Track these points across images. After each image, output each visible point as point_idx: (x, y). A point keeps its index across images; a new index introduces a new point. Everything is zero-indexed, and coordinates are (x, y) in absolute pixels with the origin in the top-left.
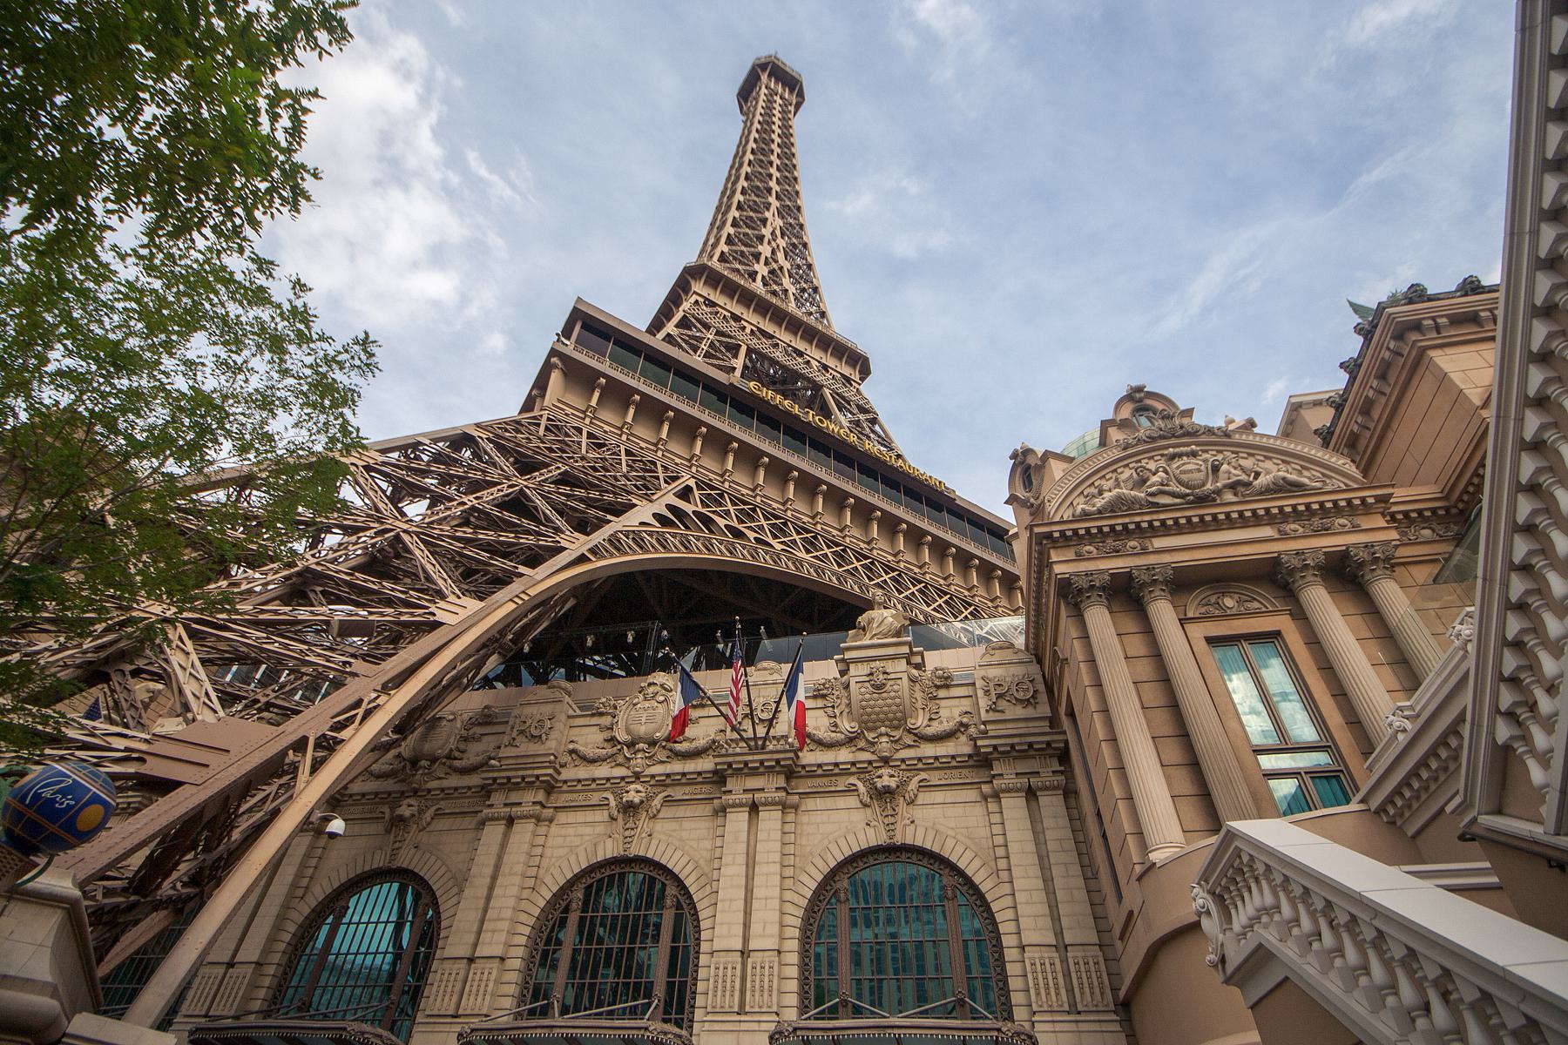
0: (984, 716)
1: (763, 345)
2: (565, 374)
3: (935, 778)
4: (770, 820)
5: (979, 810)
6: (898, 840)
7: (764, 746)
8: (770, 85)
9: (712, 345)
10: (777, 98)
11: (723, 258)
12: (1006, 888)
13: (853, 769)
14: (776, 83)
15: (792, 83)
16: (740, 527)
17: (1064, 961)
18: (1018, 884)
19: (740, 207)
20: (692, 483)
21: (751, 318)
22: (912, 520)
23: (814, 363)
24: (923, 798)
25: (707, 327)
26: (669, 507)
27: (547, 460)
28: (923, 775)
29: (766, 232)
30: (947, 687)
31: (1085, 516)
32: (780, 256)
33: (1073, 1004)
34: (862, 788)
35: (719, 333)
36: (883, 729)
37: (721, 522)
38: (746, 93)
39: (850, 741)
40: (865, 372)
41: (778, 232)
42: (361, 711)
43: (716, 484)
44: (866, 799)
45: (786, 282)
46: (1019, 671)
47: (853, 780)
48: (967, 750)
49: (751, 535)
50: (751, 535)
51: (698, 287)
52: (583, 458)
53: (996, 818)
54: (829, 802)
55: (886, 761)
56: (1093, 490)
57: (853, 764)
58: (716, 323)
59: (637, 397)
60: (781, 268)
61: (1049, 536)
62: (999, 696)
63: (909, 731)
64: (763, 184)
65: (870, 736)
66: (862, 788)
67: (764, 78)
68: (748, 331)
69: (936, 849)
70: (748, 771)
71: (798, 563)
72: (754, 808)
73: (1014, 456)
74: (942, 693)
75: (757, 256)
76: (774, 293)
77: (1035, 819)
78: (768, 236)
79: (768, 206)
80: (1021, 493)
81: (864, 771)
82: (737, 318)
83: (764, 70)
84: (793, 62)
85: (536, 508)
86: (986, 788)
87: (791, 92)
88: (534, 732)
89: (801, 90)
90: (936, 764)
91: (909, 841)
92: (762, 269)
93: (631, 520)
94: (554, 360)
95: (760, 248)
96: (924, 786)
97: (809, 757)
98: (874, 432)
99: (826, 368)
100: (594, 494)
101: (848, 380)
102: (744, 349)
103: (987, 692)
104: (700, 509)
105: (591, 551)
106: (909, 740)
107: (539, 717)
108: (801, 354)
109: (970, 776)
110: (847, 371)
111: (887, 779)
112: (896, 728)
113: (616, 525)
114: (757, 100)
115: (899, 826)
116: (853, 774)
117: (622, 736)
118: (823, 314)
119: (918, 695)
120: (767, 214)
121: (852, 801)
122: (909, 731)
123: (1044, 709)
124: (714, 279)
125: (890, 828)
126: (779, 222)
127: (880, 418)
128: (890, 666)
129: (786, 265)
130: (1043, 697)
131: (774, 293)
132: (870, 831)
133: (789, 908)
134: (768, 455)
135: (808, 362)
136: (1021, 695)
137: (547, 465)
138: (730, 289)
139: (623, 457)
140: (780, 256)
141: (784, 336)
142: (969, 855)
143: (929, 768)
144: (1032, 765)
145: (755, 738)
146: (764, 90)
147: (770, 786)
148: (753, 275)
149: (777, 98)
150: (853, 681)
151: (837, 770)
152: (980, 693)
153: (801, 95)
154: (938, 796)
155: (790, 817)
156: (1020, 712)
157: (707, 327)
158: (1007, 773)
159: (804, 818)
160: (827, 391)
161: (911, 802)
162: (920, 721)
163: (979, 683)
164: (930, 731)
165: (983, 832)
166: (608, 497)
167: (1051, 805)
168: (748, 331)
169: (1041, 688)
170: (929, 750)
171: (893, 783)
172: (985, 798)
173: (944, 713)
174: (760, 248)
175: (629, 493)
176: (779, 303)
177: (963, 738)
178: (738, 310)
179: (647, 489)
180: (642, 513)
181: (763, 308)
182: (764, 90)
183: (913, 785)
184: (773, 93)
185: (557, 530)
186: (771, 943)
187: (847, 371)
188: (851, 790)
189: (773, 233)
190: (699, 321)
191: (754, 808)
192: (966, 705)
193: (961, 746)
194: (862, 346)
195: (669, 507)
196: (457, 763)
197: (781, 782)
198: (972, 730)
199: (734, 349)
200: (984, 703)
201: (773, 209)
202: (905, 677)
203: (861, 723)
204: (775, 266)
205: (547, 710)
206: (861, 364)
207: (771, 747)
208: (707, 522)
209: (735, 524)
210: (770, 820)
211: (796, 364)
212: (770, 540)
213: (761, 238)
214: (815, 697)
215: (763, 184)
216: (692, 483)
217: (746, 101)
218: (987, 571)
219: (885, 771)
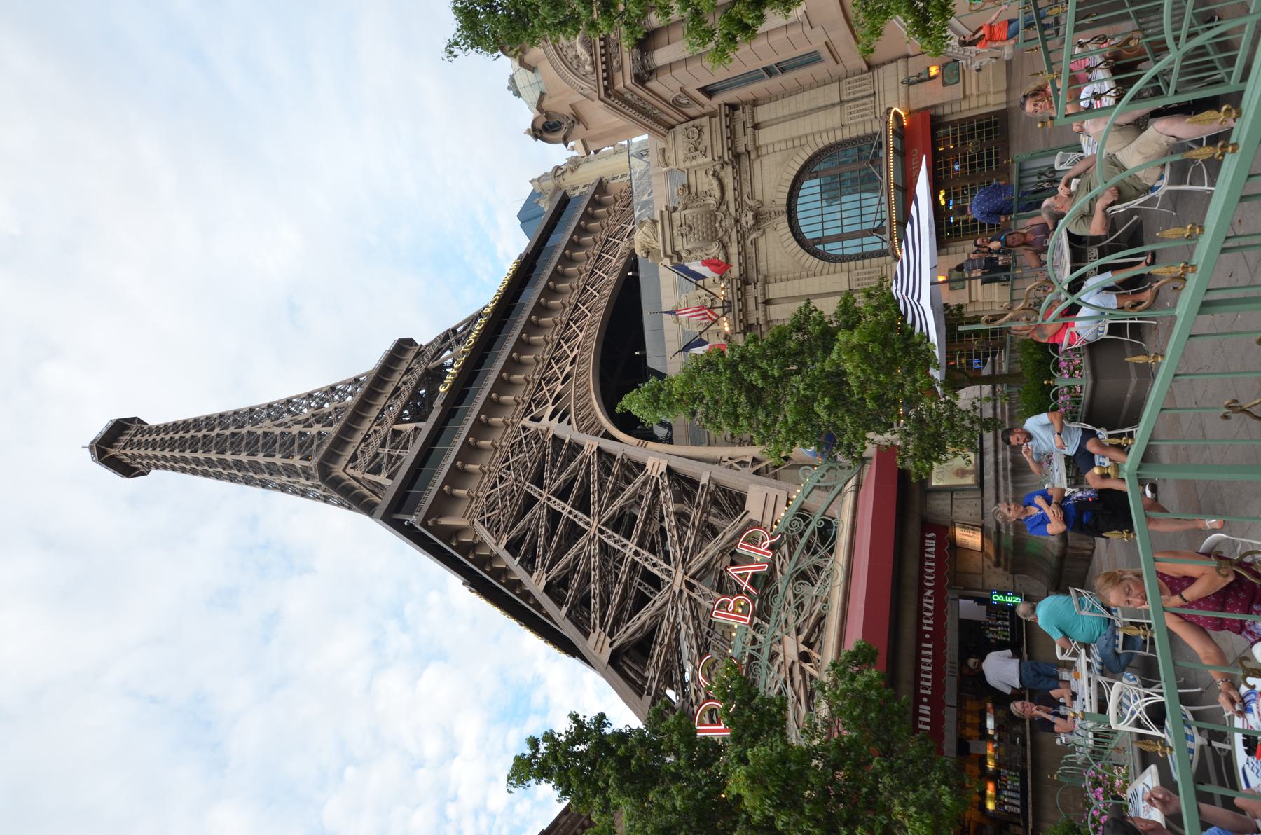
0: (709, 159)
2: (440, 517)
3: (747, 189)
4: (774, 291)
5: (765, 160)
6: (784, 208)
8: (123, 447)
10: (135, 440)
12: (811, 138)
14: (118, 441)
15: (119, 429)
17: (848, 101)
18: (808, 131)
22: (546, 279)
23: (405, 378)
24: (758, 196)
25: (377, 454)
28: (745, 197)
29: (277, 431)
30: (689, 187)
31: (594, 63)
33: (870, 96)
34: (754, 236)
35: (383, 445)
38: (128, 470)
39: (724, 247)
40: (410, 342)
42: (733, 462)
43: (526, 406)
44: (760, 232)
46: (680, 138)
47: (748, 242)
48: (729, 169)
51: (338, 470)
53: (771, 149)
54: (762, 256)
55: (737, 221)
56: (575, 62)
59: (459, 463)
61: (606, 89)
62: (696, 149)
63: (718, 208)
64: (224, 446)
65: (721, 233)
66: (754, 236)
67: (113, 452)
69: (789, 184)
70: (744, 310)
71: (587, 337)
72: (767, 302)
73: (536, 137)
74: (693, 190)
77: (771, 123)
78: (283, 429)
80: (561, 135)
81: (743, 236)
83: (105, 452)
84: (97, 427)
85: (565, 481)
86: (753, 156)
87: (129, 428)
90: (738, 189)
91: (785, 201)
94: (430, 523)
96: (751, 197)
97: (735, 271)
99: (408, 371)
100: (548, 458)
102: (397, 427)
103: (694, 158)
106: (724, 208)
108: (397, 389)
109: (745, 162)
110: (411, 355)
111: (748, 219)
112: (716, 216)
114: (134, 457)
115: (776, 209)
118: (356, 380)
119: (695, 204)
120: (260, 432)
121: (761, 242)
122: (718, 208)
123: (705, 120)
124: (332, 455)
125: (777, 214)
127: (451, 326)
128: (677, 223)
130: (697, 122)
132: (780, 227)
133: (825, 271)
134: (490, 393)
135: (404, 383)
136: (696, 136)
142: (792, 164)
143: (741, 194)
144: (739, 128)
145: (723, 307)
146: (128, 451)
147: (753, 292)
149: (135, 440)
150: (687, 247)
151: (742, 253)
152: (694, 163)
153: (132, 420)
154: (758, 187)
155: (772, 280)
156: (706, 136)
158: (743, 142)
159: (772, 271)
160: (431, 365)
161: (762, 203)
162: (712, 201)
163: (688, 164)
164: (717, 194)
165: (779, 157)
167: (763, 114)
169: (691, 123)
170: (730, 194)
171: (751, 214)
172: (759, 156)
173: (706, 188)
176: (328, 442)
177: (722, 174)
178: (359, 437)
182: (128, 451)
183: (751, 203)
184: (130, 444)
186: (845, 277)
187: (411, 355)
188: (754, 242)
190: (371, 462)
191: (767, 302)
192: (701, 174)
193: (728, 174)
194: (387, 345)
197: (750, 288)
198: (718, 168)
199: (396, 433)
200: (701, 160)
201: (253, 429)
202: (684, 212)
203: (713, 240)
204: (312, 420)
206: (404, 346)
208: (559, 397)
209: (560, 381)
210: (774, 291)
211: (406, 392)
215: (224, 446)
217: (135, 469)
218: (588, 217)
219: (743, 220)
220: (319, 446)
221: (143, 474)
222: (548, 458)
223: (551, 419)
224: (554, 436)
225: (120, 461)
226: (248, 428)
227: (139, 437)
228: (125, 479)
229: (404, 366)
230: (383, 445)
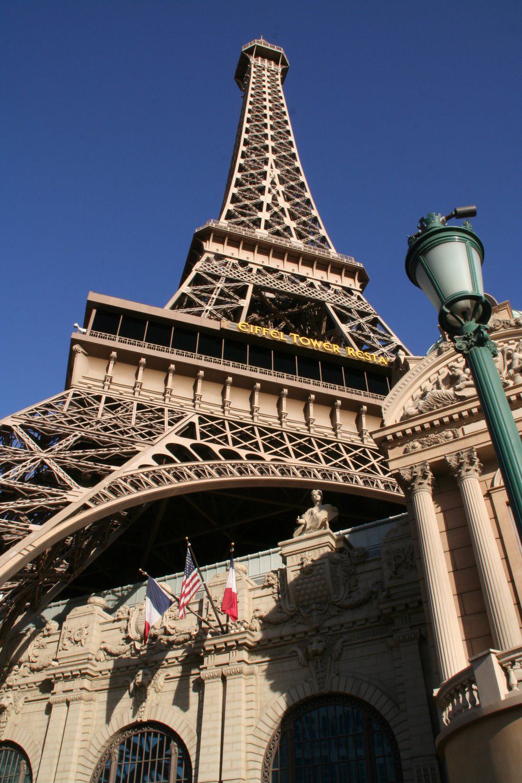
1: (270, 280)
7: (227, 631)
9: (222, 293)
10: (265, 73)
11: (230, 216)
13: (294, 640)
16: (235, 449)
19: (240, 170)
20: (195, 419)
21: (257, 259)
23: (317, 284)
25: (217, 278)
26: (170, 447)
27: (67, 431)
29: (266, 183)
32: (281, 200)
35: (228, 280)
36: (314, 606)
37: (216, 448)
41: (277, 181)
45: (287, 221)
47: (294, 648)
49: (243, 453)
50: (243, 453)
52: (98, 422)
57: (294, 635)
58: (224, 272)
60: (282, 210)
63: (334, 604)
67: (253, 60)
68: (254, 271)
74: (359, 569)
75: (259, 206)
76: (277, 233)
79: (266, 162)
82: (243, 263)
87: (277, 63)
88: (77, 638)
89: (283, 59)
92: (265, 215)
93: (131, 467)
95: (262, 198)
98: (374, 332)
99: (327, 285)
100: (104, 451)
101: (349, 291)
104: (199, 441)
105: (92, 500)
107: (79, 627)
108: (303, 279)
113: (119, 472)
116: (293, 643)
117: (133, 634)
120: (266, 168)
126: (277, 172)
129: (286, 206)
131: (277, 233)
135: (312, 285)
137: (68, 435)
138: (235, 241)
139: (135, 412)
140: (281, 200)
141: (288, 267)
145: (221, 626)
146: (253, 69)
148: (257, 223)
149: (265, 73)
157: (217, 278)
160: (329, 306)
166: (115, 451)
168: (254, 271)
174: (262, 198)
175: (133, 443)
179: (150, 435)
180: (145, 455)
181: (264, 248)
183: (338, 646)
185: (67, 488)
187: (348, 282)
189: (273, 183)
195: (170, 447)
196: (35, 666)
199: (241, 292)
201: (271, 162)
204: (276, 209)
205: (84, 621)
207: (232, 632)
209: (230, 447)
212: (262, 453)
213: (262, 190)
214: (264, 587)
216: (195, 419)
222: (104, 451)
224: (138, 452)
227: (268, 74)
229: (332, 278)
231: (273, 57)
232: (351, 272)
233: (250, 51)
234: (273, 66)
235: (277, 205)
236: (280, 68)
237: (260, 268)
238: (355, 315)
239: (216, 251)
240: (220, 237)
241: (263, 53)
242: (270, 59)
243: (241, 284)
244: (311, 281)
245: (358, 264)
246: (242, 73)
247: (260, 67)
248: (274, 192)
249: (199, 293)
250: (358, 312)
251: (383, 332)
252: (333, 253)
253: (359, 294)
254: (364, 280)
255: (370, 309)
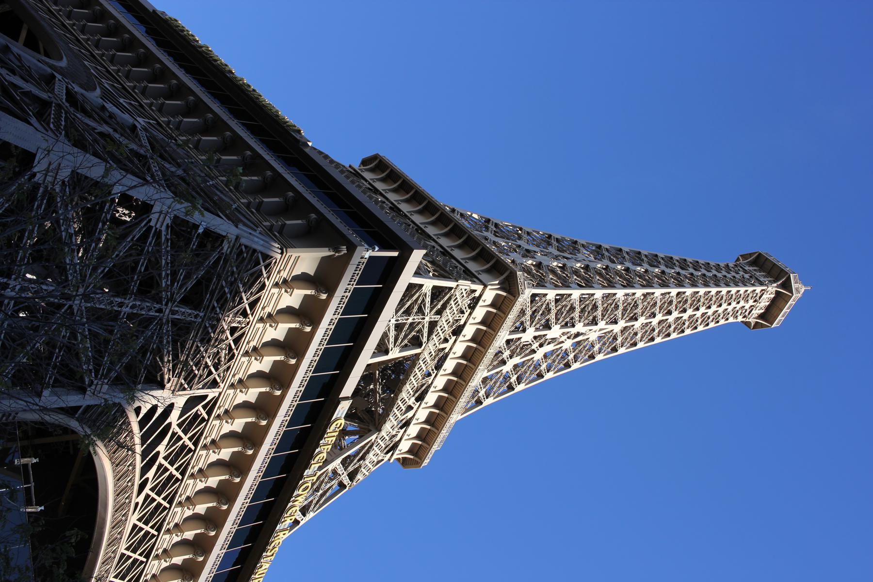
23: (410, 414)
25: (439, 312)
35: (433, 325)
87: (761, 316)
92: (528, 336)
99: (407, 424)
108: (420, 399)
120: (602, 324)
129: (538, 356)
135: (410, 408)
148: (521, 328)
160: (373, 437)
178: (469, 331)
187: (405, 446)
201: (611, 327)
217: (753, 263)
220: (523, 312)
221: (744, 257)
223: (172, 406)
225: (769, 274)
226: (617, 328)
227: (747, 306)
228: (763, 252)
229: (413, 430)
230: (433, 325)
231: (768, 315)
232: (417, 452)
233: (787, 285)
234: (756, 312)
235: (541, 345)
236: (752, 320)
237: (447, 351)
238: (351, 469)
239: (483, 298)
240: (501, 306)
241: (778, 301)
242: (768, 309)
243: (425, 339)
244: (415, 408)
245: (426, 462)
246: (762, 267)
247: (760, 297)
248: (564, 338)
249: (419, 302)
250: (360, 467)
251: (321, 502)
252: (456, 416)
253: (386, 459)
254: (404, 462)
255: (360, 477)
